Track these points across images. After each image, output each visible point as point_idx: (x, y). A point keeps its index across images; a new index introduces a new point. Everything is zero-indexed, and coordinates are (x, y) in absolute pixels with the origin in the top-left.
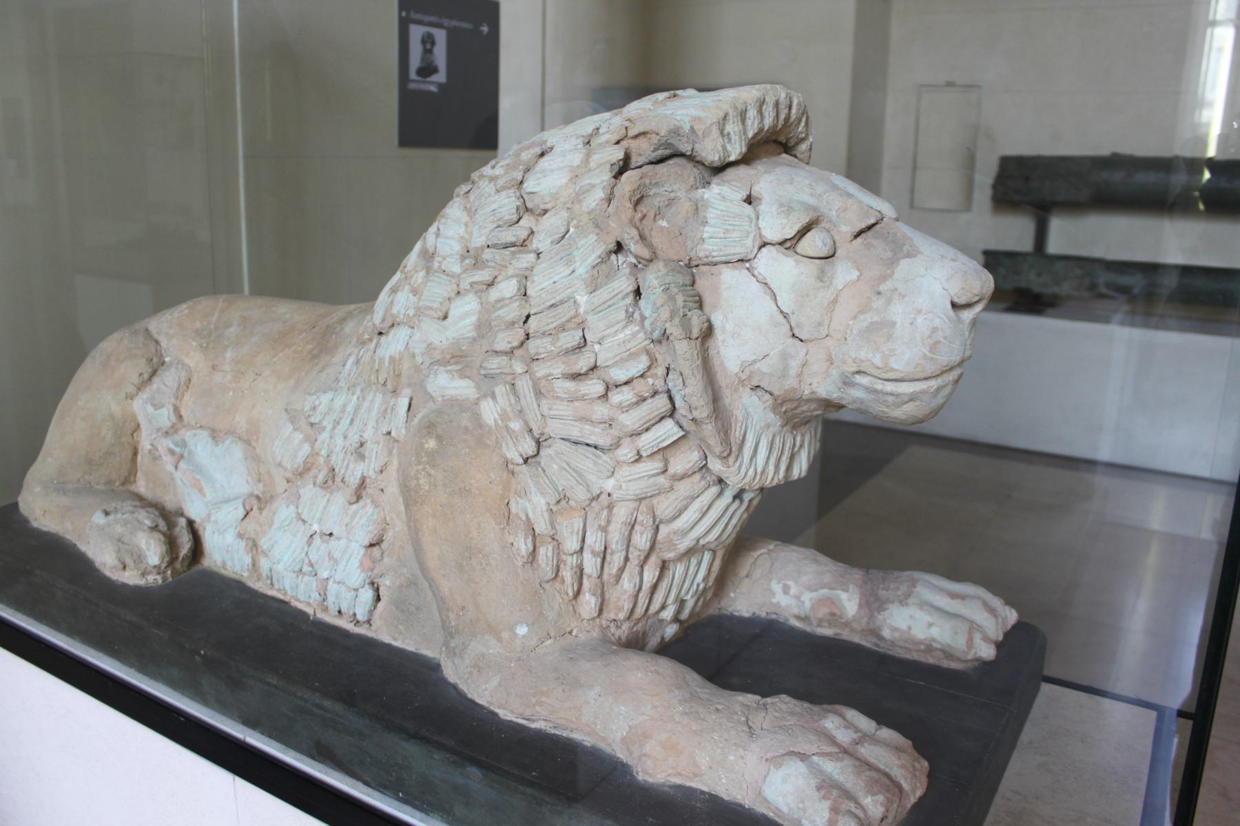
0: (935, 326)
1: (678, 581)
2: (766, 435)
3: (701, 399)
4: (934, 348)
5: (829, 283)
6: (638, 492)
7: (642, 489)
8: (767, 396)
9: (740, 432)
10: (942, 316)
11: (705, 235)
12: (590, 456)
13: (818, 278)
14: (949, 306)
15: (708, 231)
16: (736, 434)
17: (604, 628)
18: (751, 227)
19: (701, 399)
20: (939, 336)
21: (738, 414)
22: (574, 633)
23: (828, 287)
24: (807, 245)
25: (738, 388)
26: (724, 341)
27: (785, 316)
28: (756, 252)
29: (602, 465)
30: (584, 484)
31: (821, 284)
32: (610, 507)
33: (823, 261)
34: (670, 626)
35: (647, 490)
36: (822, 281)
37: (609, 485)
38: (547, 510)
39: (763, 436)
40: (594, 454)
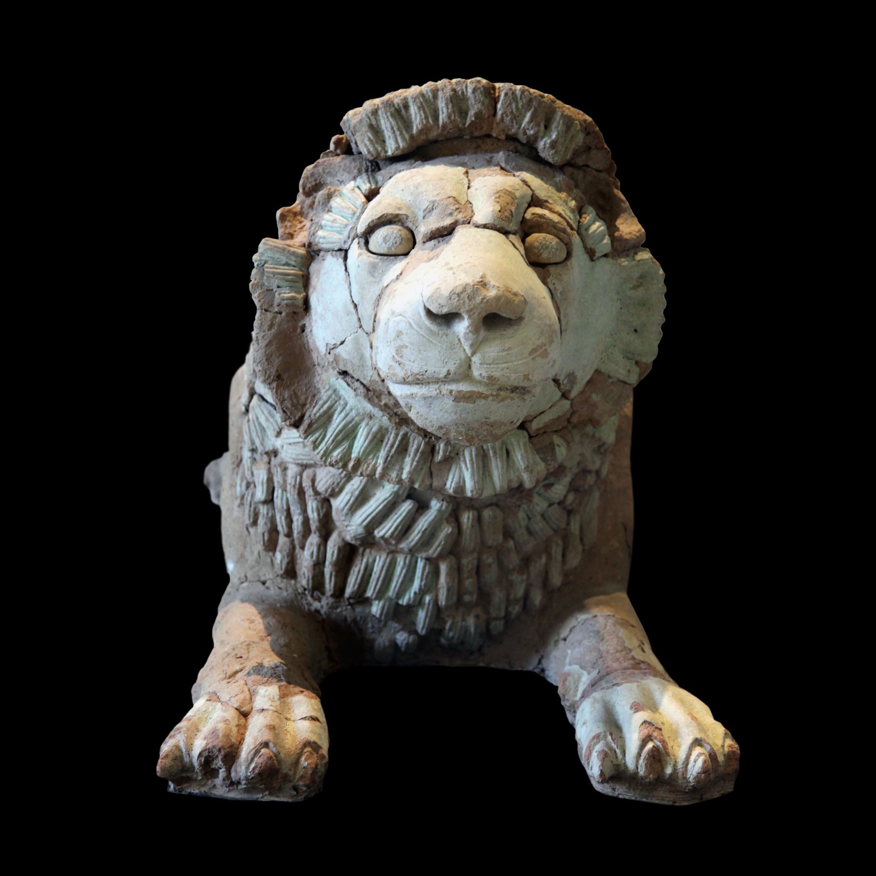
0: (400, 329)
1: (377, 576)
2: (368, 424)
3: (259, 364)
4: (399, 350)
5: (379, 279)
6: (294, 456)
7: (298, 455)
8: (357, 384)
9: (320, 409)
10: (411, 321)
11: (323, 222)
12: (266, 412)
13: (370, 272)
14: (423, 313)
15: (326, 218)
16: (314, 412)
17: (299, 594)
18: (352, 218)
19: (259, 364)
20: (405, 340)
21: (324, 395)
22: (267, 585)
23: (379, 282)
24: (378, 239)
25: (329, 368)
26: (316, 321)
27: (356, 306)
28: (349, 243)
29: (271, 423)
30: (261, 438)
31: (372, 279)
32: (285, 469)
33: (380, 257)
34: (401, 633)
35: (303, 457)
36: (373, 276)
37: (278, 443)
38: (250, 458)
39: (363, 424)
40: (269, 412)
